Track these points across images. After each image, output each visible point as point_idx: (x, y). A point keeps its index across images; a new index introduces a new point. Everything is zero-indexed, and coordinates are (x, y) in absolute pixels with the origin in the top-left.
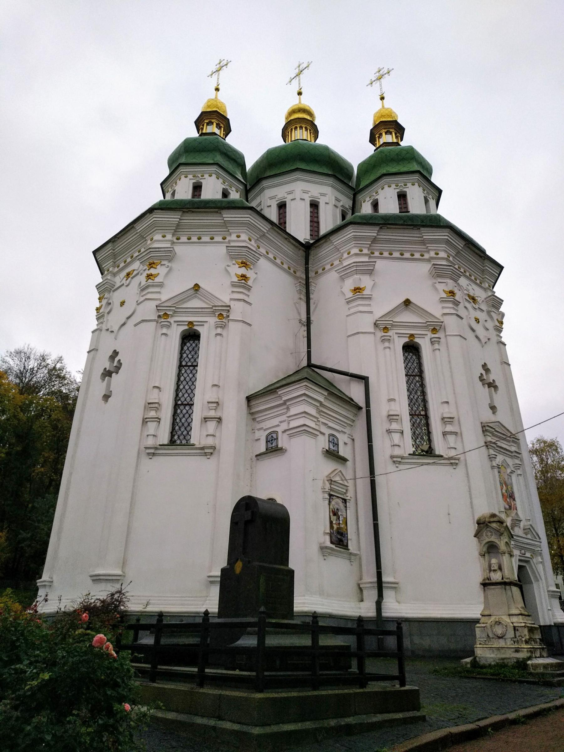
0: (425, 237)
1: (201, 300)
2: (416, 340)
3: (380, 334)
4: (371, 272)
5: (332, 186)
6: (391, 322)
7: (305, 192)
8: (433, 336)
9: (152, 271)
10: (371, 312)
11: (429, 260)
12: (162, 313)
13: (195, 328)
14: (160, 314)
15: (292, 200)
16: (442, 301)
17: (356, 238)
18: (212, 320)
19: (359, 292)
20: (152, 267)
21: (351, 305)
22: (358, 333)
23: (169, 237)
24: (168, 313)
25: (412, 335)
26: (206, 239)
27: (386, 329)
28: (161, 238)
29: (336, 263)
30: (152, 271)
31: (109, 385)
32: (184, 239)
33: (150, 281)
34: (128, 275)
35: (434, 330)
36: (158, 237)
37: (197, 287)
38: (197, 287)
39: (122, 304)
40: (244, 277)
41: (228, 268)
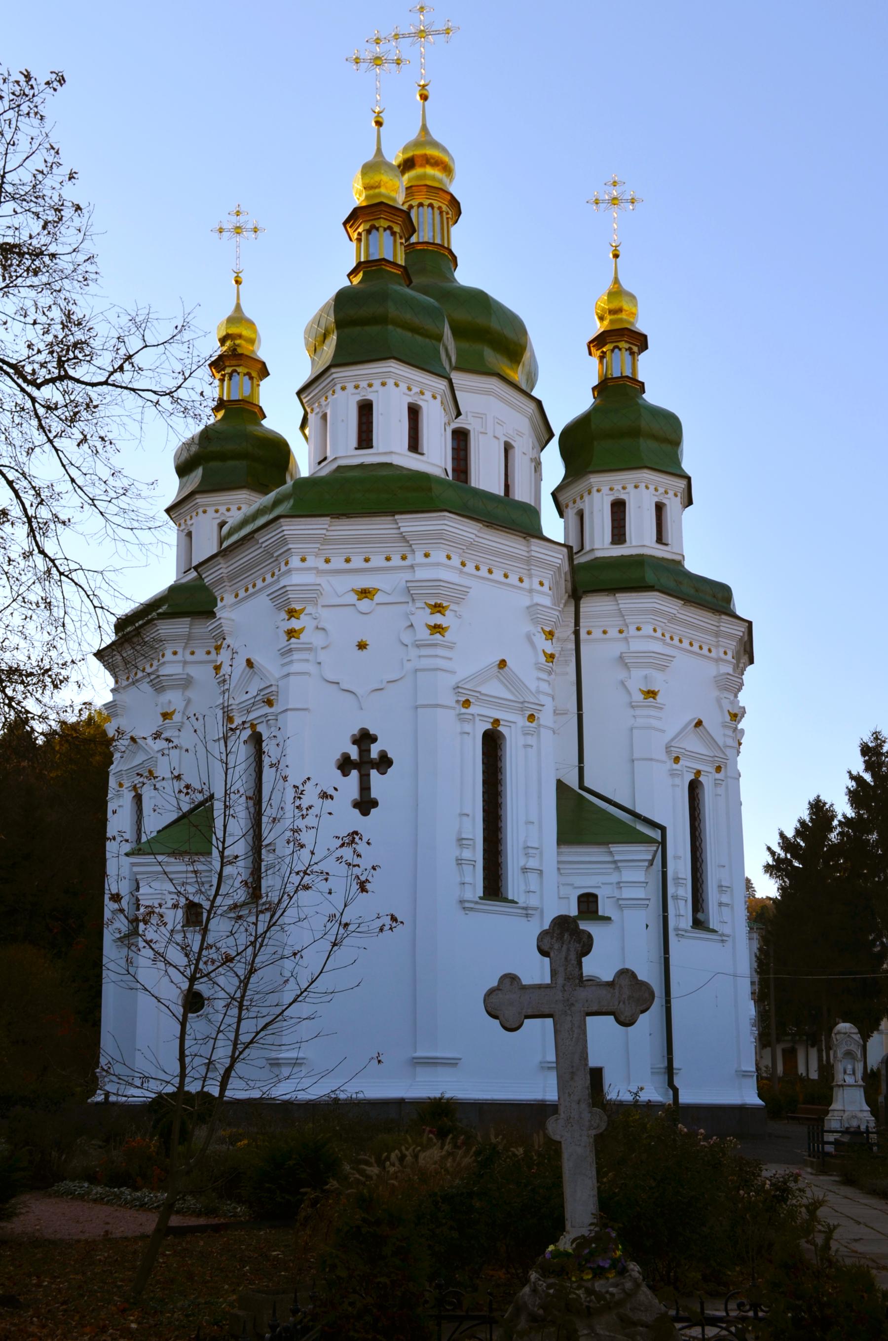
0: (722, 628)
1: (503, 683)
2: (702, 779)
3: (670, 764)
4: (663, 668)
5: (531, 419)
6: (683, 751)
7: (500, 423)
8: (718, 776)
9: (438, 619)
10: (663, 731)
11: (718, 660)
12: (464, 699)
13: (500, 728)
14: (460, 699)
15: (482, 433)
16: (724, 726)
17: (655, 612)
18: (521, 721)
19: (654, 698)
20: (439, 612)
21: (639, 712)
22: (651, 759)
23: (456, 561)
24: (471, 700)
25: (698, 773)
26: (498, 575)
27: (677, 760)
28: (444, 560)
29: (613, 633)
30: (438, 619)
31: (365, 786)
32: (470, 568)
33: (438, 636)
34: (365, 593)
35: (718, 769)
36: (438, 556)
37: (503, 664)
38: (503, 664)
39: (362, 646)
40: (552, 656)
41: (533, 637)
